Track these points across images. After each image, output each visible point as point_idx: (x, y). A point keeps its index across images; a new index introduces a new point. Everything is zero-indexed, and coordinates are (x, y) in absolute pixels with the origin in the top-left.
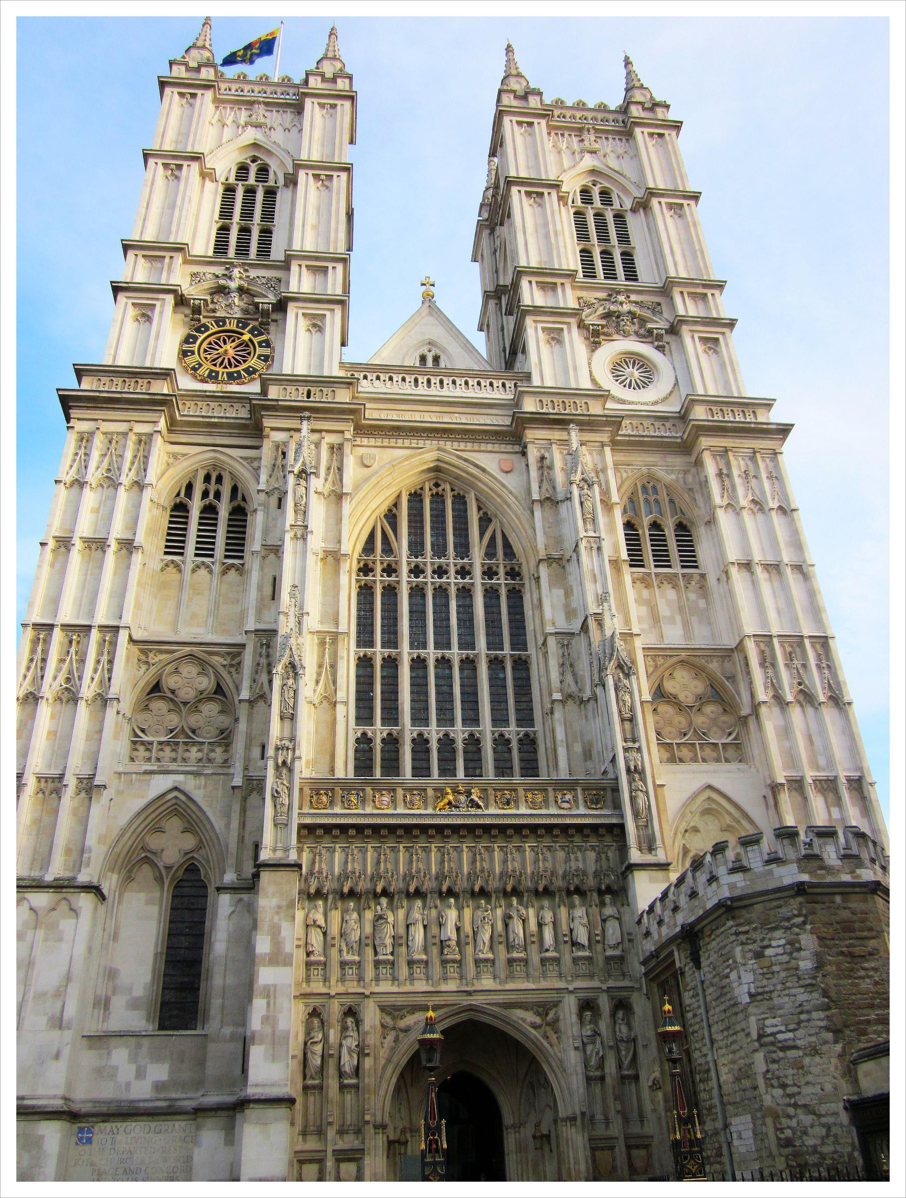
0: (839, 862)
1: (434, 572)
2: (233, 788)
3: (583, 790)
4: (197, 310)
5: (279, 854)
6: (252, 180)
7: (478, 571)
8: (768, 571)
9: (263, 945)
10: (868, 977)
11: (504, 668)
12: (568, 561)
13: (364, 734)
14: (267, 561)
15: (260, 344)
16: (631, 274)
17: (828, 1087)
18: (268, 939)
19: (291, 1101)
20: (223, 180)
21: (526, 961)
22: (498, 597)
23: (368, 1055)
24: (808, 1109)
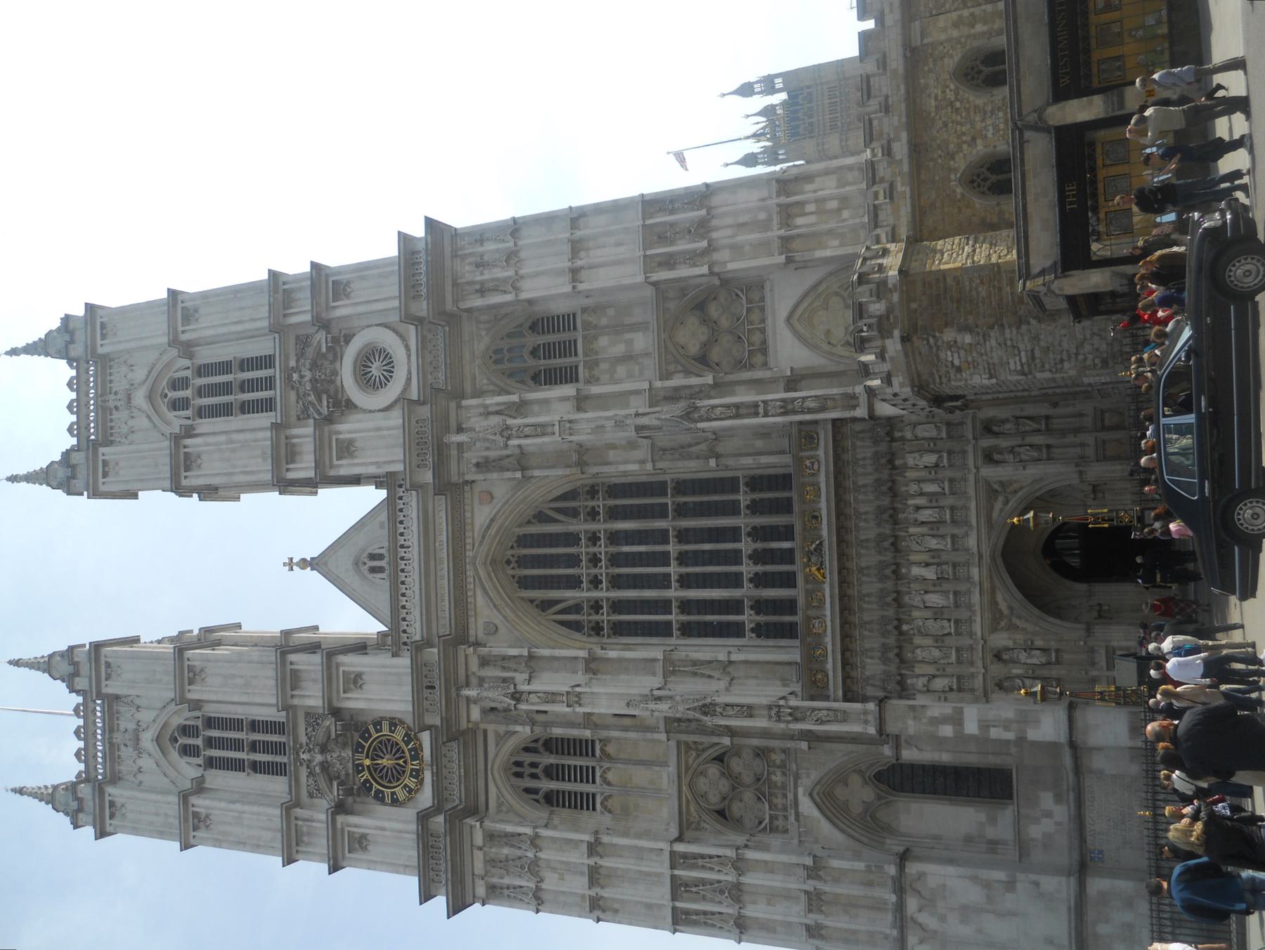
0: (883, 301)
1: (596, 566)
2: (809, 748)
3: (802, 450)
4: (349, 792)
5: (870, 718)
6: (199, 742)
7: (593, 526)
8: (578, 252)
9: (947, 731)
10: (976, 289)
11: (685, 503)
12: (581, 446)
13: (752, 630)
14: (598, 722)
15: (377, 731)
16: (267, 362)
17: (1063, 332)
18: (941, 727)
19: (1071, 707)
20: (202, 769)
21: (952, 508)
22: (616, 506)
23: (1032, 642)
24: (1080, 345)
